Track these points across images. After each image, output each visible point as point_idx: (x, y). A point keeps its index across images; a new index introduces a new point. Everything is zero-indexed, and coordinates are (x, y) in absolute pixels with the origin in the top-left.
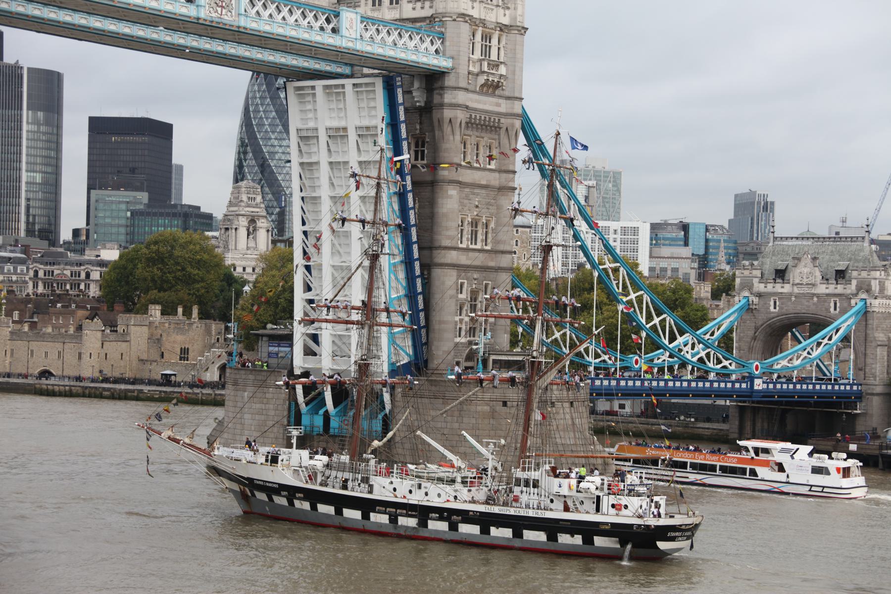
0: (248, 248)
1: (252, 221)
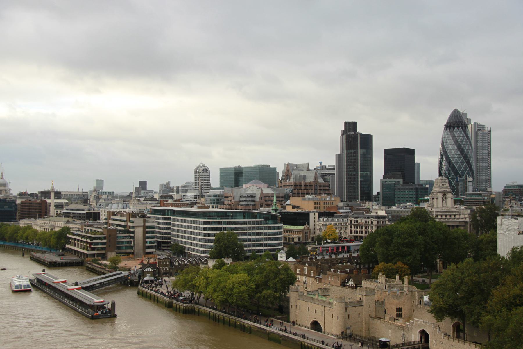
0: (443, 207)
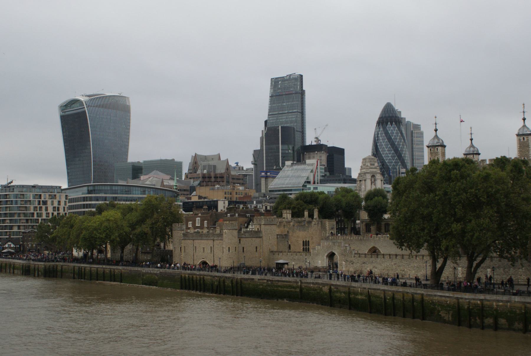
1: (373, 176)
